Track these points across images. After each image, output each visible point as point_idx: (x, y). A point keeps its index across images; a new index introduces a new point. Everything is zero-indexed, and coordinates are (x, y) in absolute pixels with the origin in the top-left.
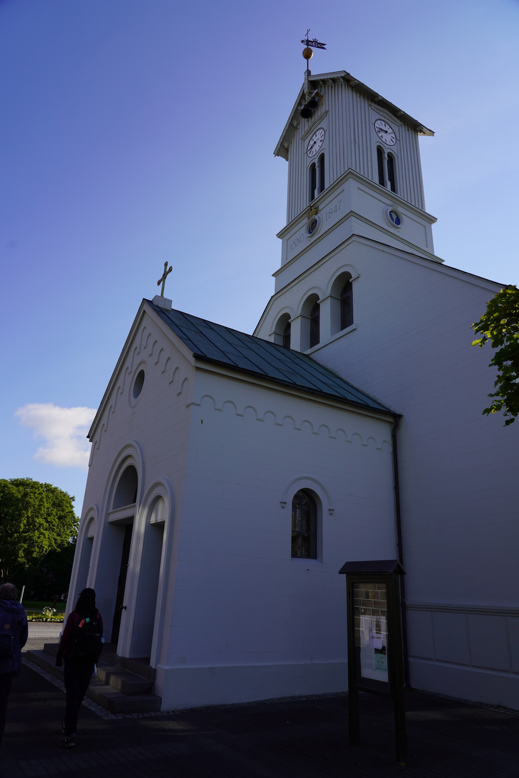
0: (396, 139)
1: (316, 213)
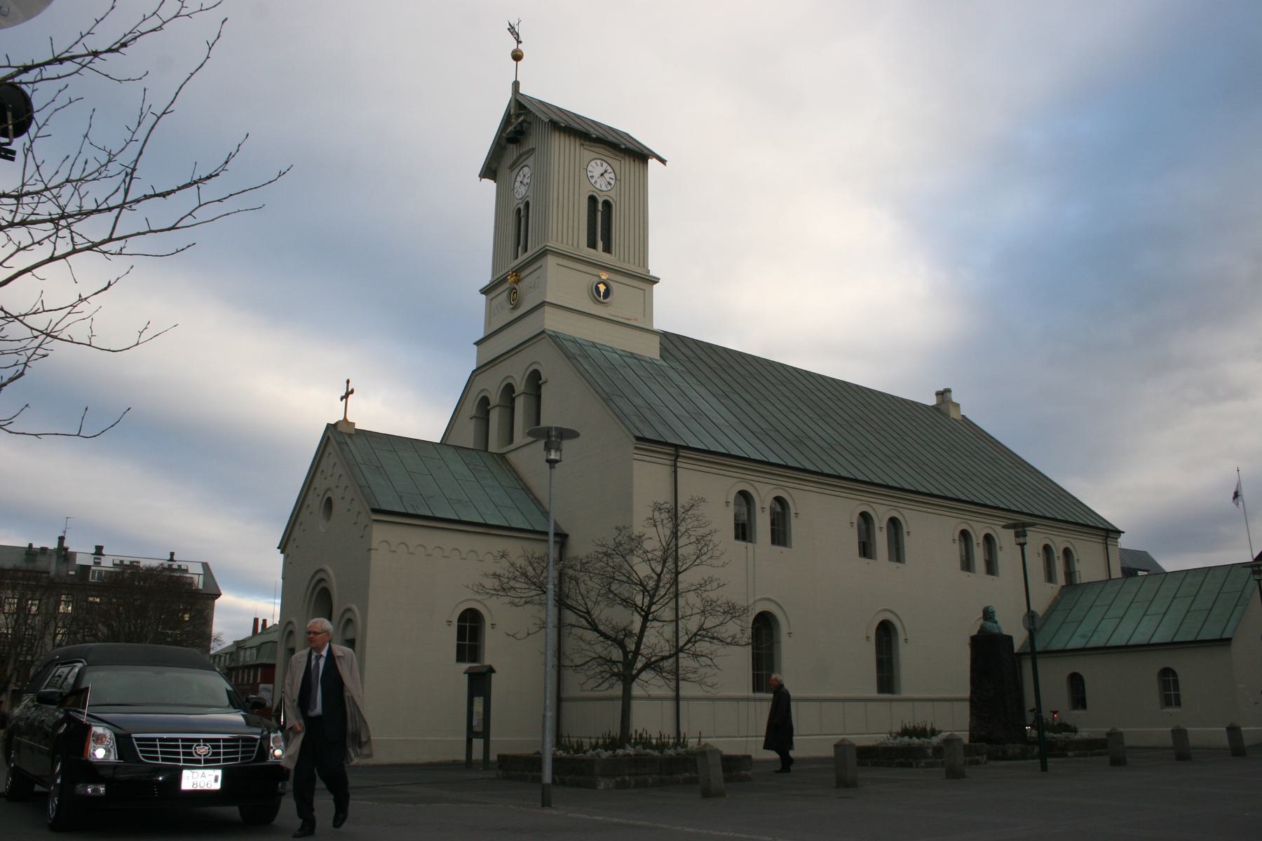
1: (517, 282)
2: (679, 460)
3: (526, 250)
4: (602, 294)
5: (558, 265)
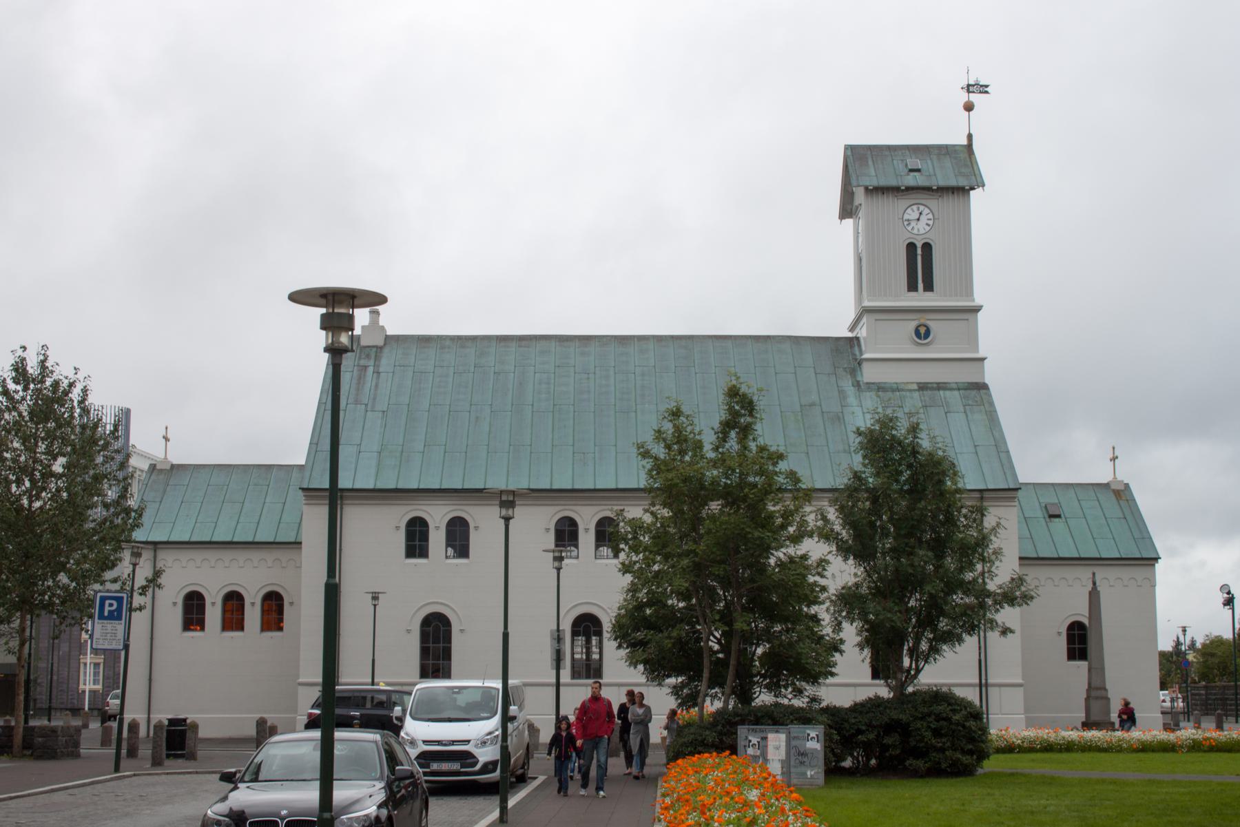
4: (922, 335)
5: (876, 320)
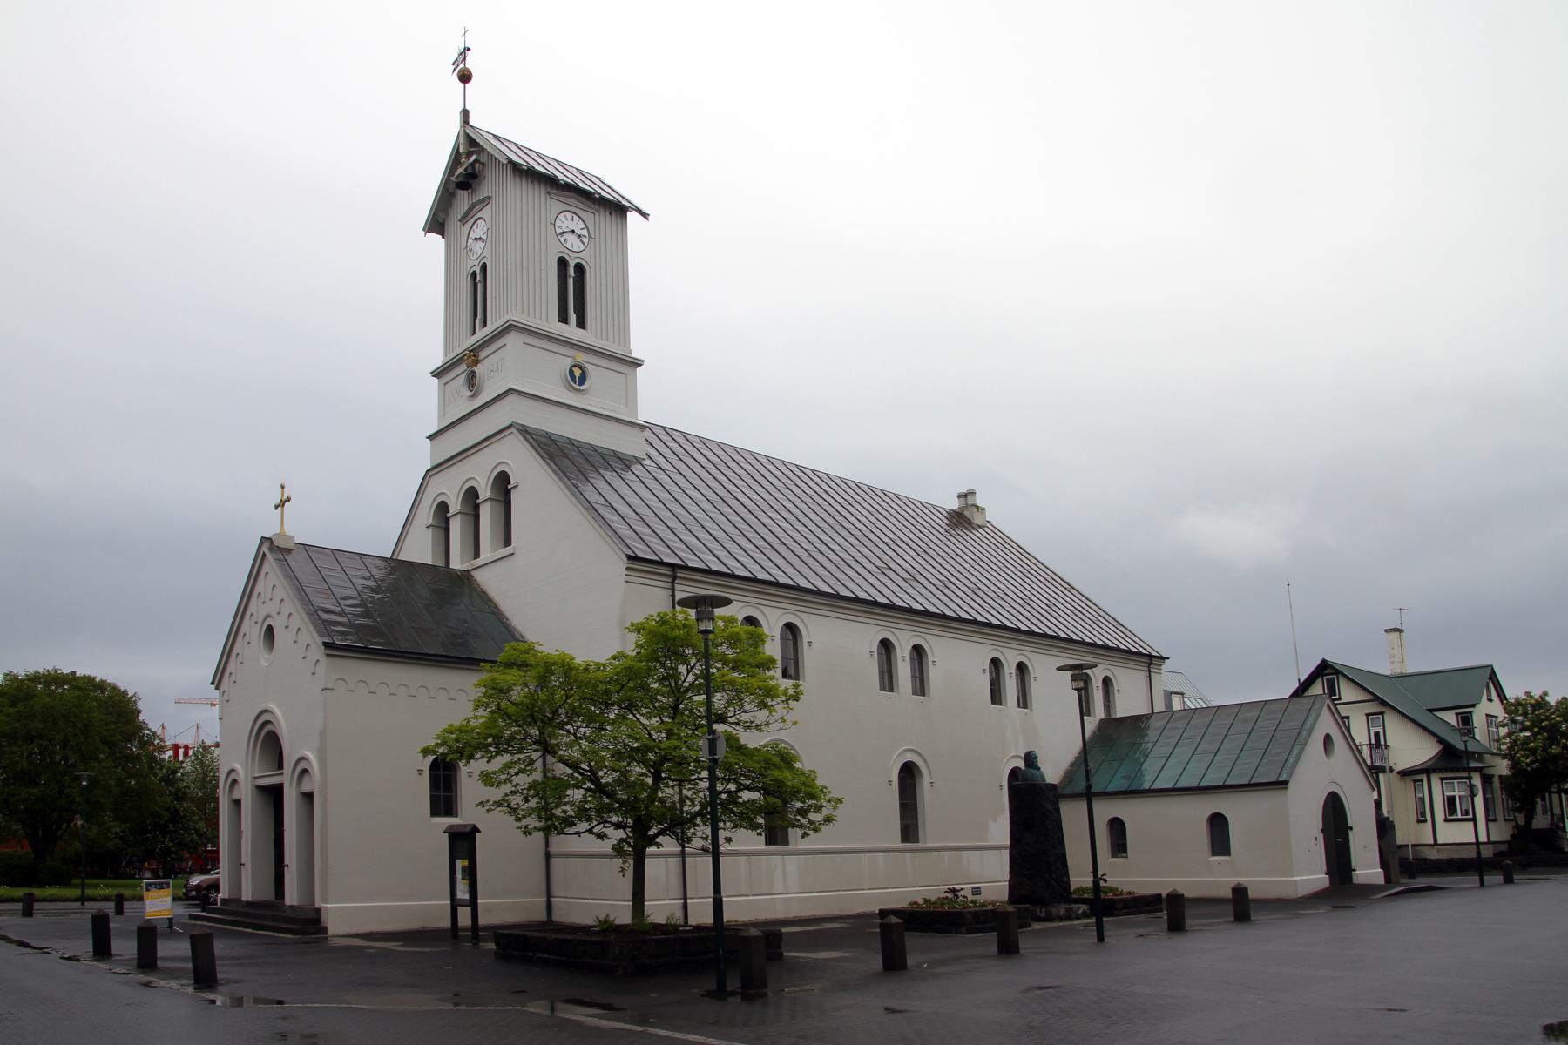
0: (590, 237)
1: (476, 363)
2: (676, 581)
3: (485, 324)
4: (577, 379)
5: (524, 343)
